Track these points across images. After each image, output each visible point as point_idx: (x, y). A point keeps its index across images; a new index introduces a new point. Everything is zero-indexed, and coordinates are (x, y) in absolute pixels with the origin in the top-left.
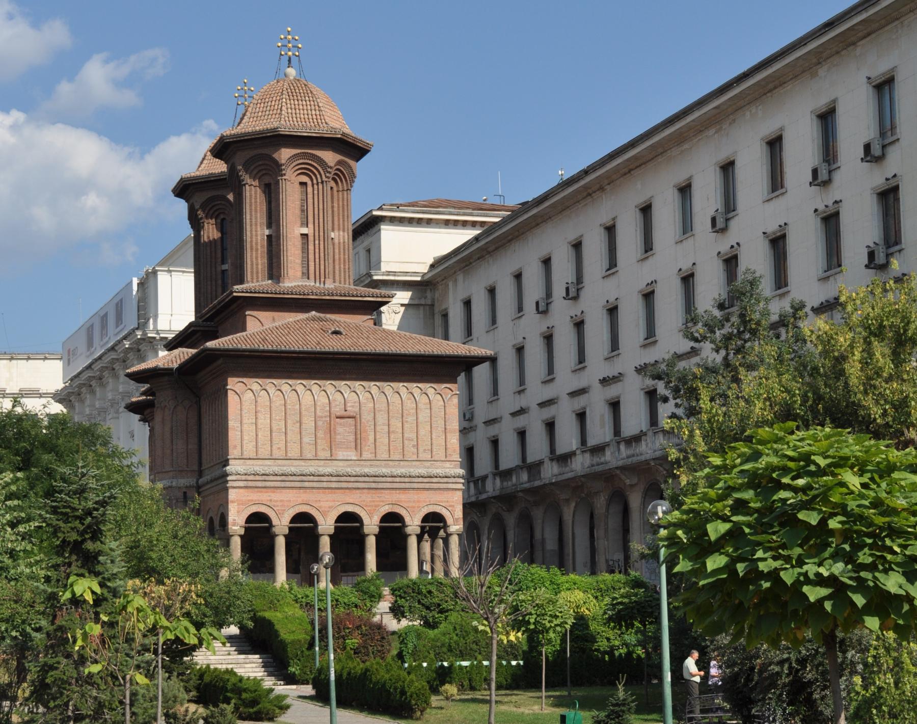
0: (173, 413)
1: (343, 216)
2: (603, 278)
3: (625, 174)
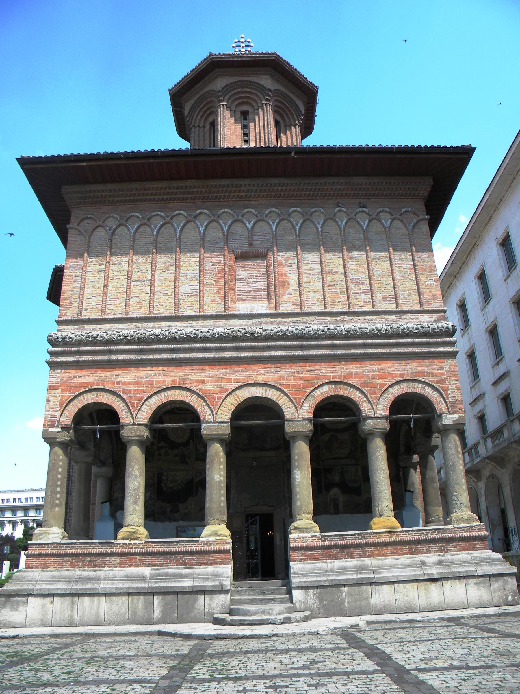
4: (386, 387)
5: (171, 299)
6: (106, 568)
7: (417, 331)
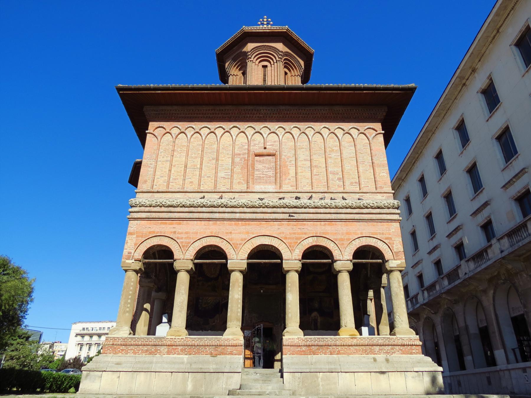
2: (487, 121)
4: (351, 241)
5: (212, 180)
6: (158, 355)
7: (373, 205)
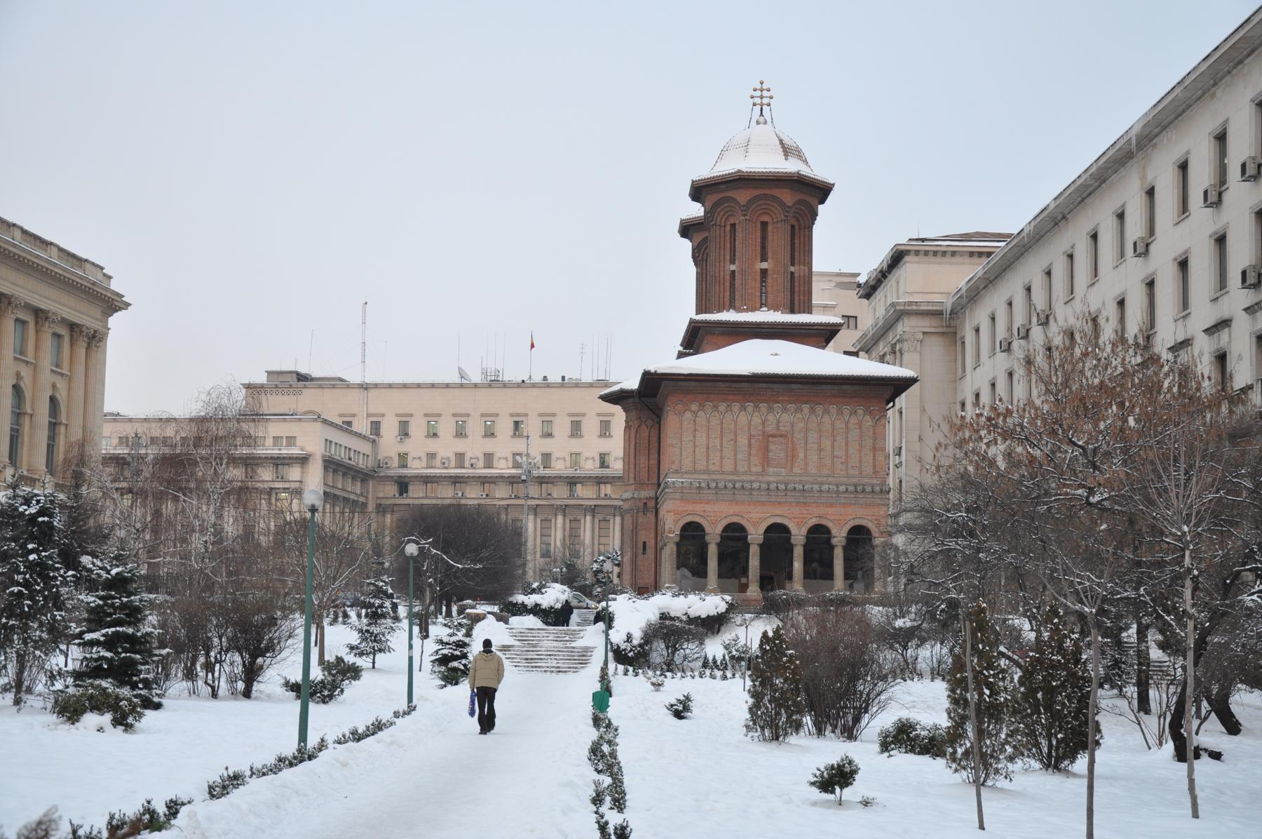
0: (636, 432)
1: (804, 251)
3: (1080, 203)
